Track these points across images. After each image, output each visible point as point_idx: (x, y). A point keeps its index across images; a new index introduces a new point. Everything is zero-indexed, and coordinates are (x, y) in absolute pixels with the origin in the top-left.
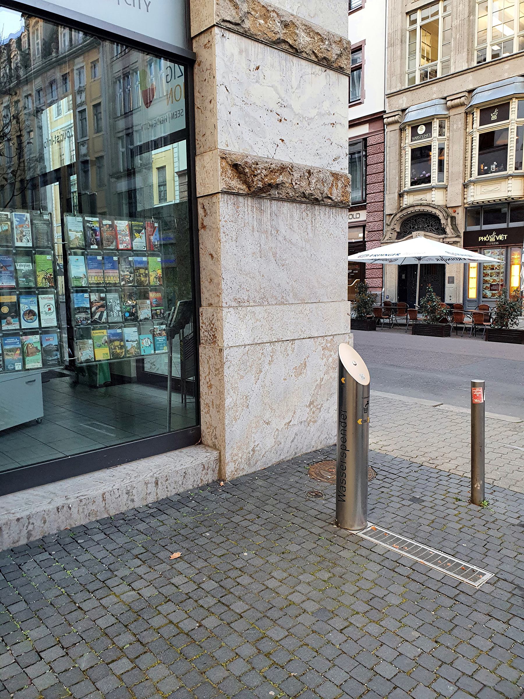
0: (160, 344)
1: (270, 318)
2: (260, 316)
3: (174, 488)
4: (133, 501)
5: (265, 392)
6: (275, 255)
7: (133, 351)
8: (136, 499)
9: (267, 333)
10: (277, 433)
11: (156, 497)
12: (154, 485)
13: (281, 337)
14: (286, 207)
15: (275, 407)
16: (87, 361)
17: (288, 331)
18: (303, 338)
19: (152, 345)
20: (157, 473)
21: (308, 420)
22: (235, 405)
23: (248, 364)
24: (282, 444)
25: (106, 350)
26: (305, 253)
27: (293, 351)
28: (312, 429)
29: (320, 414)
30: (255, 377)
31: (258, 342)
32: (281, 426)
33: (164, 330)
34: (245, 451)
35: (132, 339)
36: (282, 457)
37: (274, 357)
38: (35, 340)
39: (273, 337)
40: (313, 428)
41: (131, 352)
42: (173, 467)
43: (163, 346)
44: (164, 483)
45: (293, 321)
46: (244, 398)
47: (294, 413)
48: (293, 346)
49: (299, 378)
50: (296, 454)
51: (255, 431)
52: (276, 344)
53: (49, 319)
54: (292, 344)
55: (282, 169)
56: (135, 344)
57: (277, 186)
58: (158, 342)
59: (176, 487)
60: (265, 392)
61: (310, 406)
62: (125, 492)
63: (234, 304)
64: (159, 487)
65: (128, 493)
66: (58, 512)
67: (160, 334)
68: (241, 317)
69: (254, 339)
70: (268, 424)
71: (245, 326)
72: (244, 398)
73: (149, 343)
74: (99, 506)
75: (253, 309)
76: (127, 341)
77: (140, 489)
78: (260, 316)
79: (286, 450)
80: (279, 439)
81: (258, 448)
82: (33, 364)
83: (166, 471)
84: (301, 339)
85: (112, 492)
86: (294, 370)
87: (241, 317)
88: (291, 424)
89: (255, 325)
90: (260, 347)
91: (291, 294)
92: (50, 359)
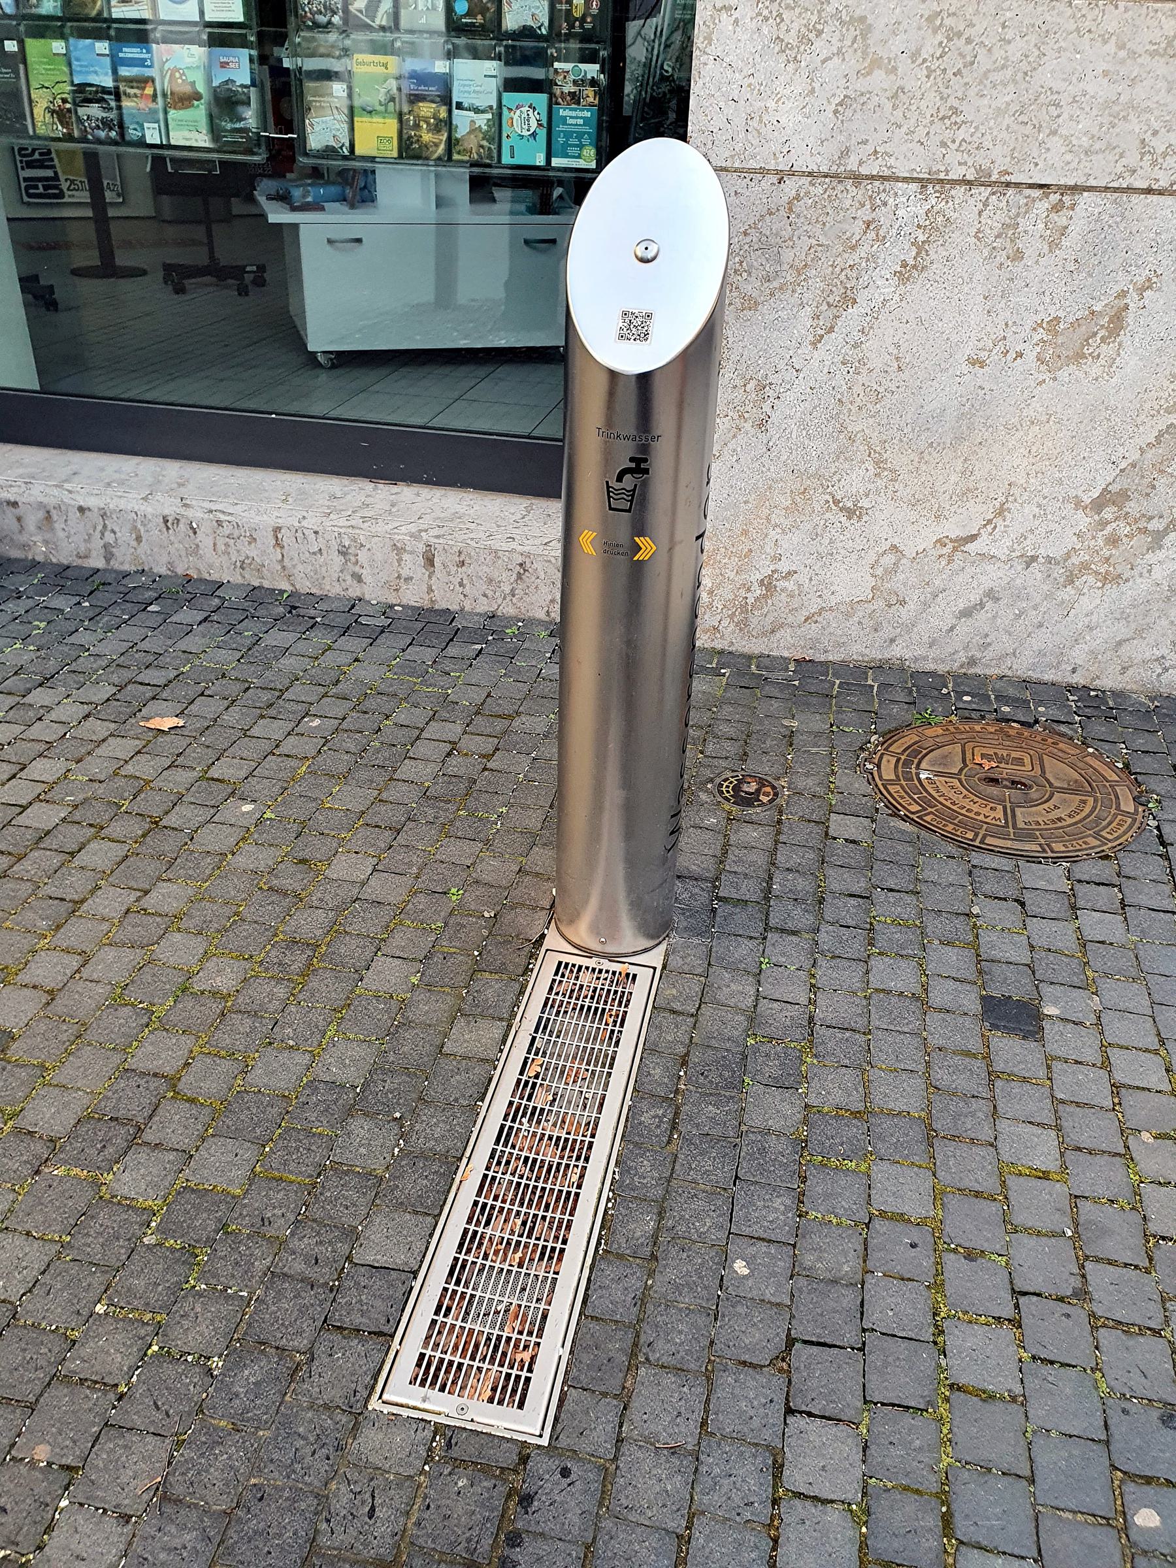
0: (568, 135)
1: (953, 62)
2: (897, 44)
3: (485, 595)
4: (358, 578)
5: (858, 389)
7: (472, 143)
8: (367, 578)
9: (921, 132)
10: (889, 560)
11: (427, 597)
12: (421, 561)
13: (1002, 163)
15: (898, 459)
16: (329, 152)
17: (1055, 143)
18: (1149, 191)
19: (542, 133)
20: (432, 533)
21: (1075, 560)
23: (788, 255)
24: (911, 606)
27: (1053, 245)
28: (1086, 604)
29: (1150, 557)
30: (817, 317)
31: (864, 171)
32: (921, 537)
33: (593, 82)
34: (732, 575)
35: (477, 103)
36: (897, 651)
37: (936, 253)
38: (189, 61)
39: (953, 158)
40: (1091, 601)
41: (467, 145)
42: (482, 535)
43: (581, 146)
44: (453, 569)
45: (1099, 89)
46: (751, 386)
47: (1001, 512)
48: (1061, 219)
49: (1063, 375)
50: (972, 662)
51: (786, 523)
52: (959, 192)
54: (1057, 208)
56: (482, 120)
58: (561, 128)
59: (490, 594)
60: (858, 389)
61: (1098, 505)
62: (335, 546)
64: (438, 574)
65: (343, 552)
66: (168, 528)
67: (575, 98)
68: (792, 38)
69: (845, 153)
70: (850, 513)
71: (801, 85)
72: (751, 386)
73: (534, 125)
74: (264, 553)
76: (459, 106)
77: (379, 556)
78: (897, 44)
79: (923, 631)
80: (896, 582)
81: (790, 585)
82: (186, 134)
83: (460, 536)
84: (1130, 190)
85: (299, 534)
86: (1041, 334)
87: (792, 38)
88: (970, 547)
89: (861, 84)
90: (860, 194)
92: (229, 126)
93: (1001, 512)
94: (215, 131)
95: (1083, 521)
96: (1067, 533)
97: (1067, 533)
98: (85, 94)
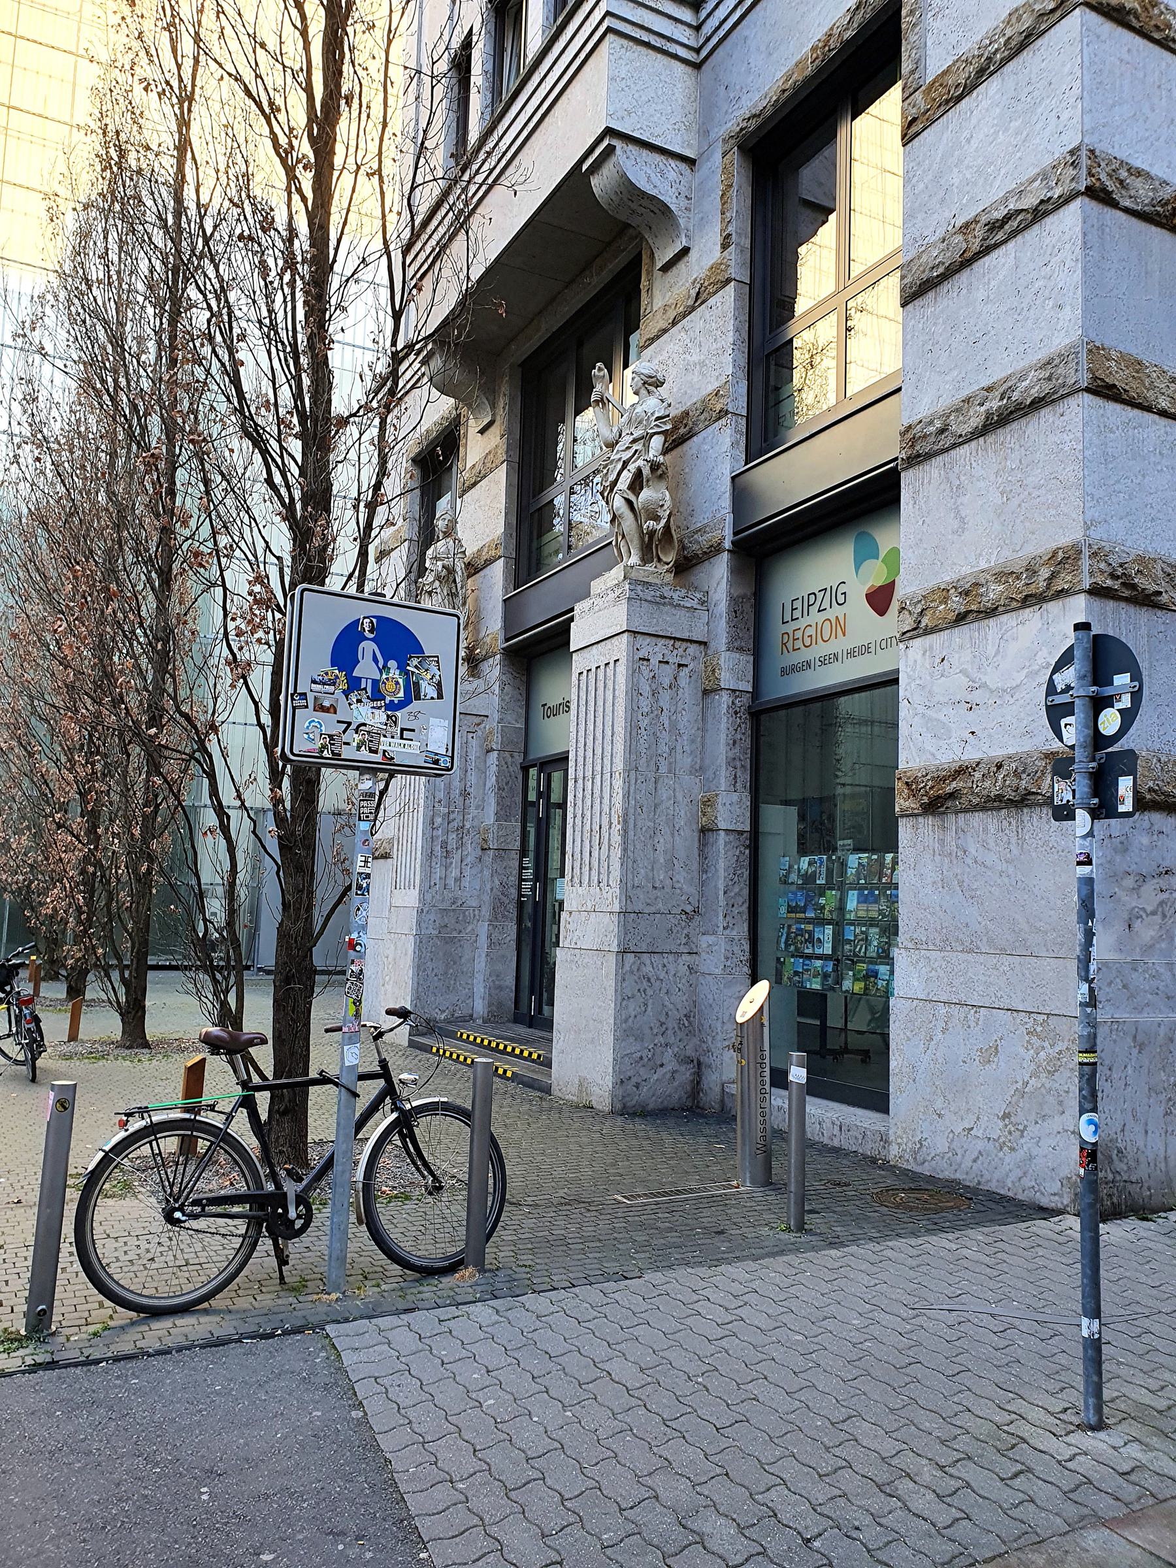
2: (937, 964)
6: (961, 883)
14: (977, 819)
22: (901, 1072)
25: (862, 985)
26: (1006, 880)
36: (958, 1176)
40: (1009, 1159)
53: (827, 949)
55: (961, 771)
57: (952, 796)
63: (910, 945)
75: (928, 954)
78: (937, 964)
91: (985, 939)
93: (978, 1118)
94: (823, 984)
95: (1001, 1124)
96: (997, 1129)
97: (997, 1129)
98: (796, 973)
